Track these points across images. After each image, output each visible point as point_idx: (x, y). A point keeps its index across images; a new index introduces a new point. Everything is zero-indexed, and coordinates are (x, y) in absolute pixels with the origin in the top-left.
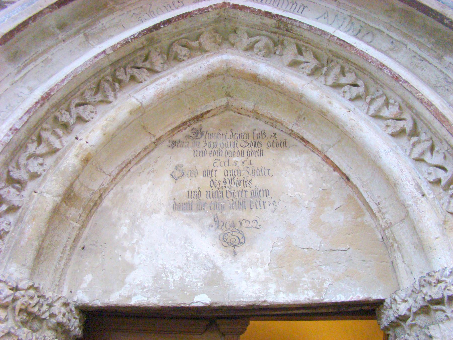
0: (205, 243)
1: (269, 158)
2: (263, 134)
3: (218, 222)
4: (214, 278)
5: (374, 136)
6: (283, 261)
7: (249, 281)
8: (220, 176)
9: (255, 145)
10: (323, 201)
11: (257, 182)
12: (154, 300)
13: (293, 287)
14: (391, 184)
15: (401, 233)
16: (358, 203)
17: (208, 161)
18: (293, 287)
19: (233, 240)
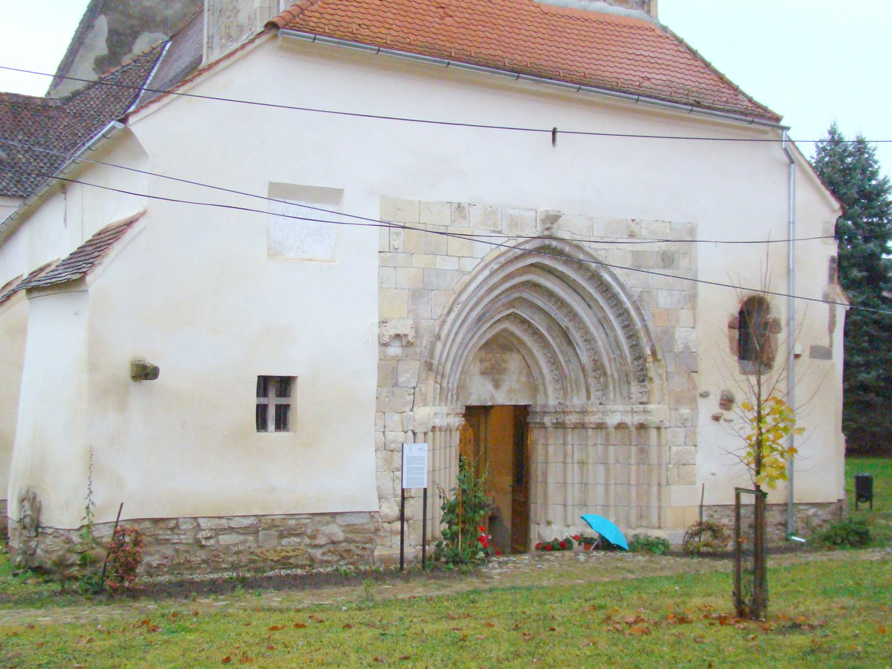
0: (490, 387)
1: (507, 356)
2: (505, 345)
3: (493, 380)
4: (492, 397)
5: (543, 362)
6: (511, 391)
7: (502, 398)
8: (493, 362)
9: (504, 349)
10: (520, 373)
11: (503, 365)
12: (478, 404)
13: (511, 400)
14: (543, 378)
15: (541, 388)
16: (530, 375)
17: (490, 356)
18: (511, 400)
19: (497, 385)
